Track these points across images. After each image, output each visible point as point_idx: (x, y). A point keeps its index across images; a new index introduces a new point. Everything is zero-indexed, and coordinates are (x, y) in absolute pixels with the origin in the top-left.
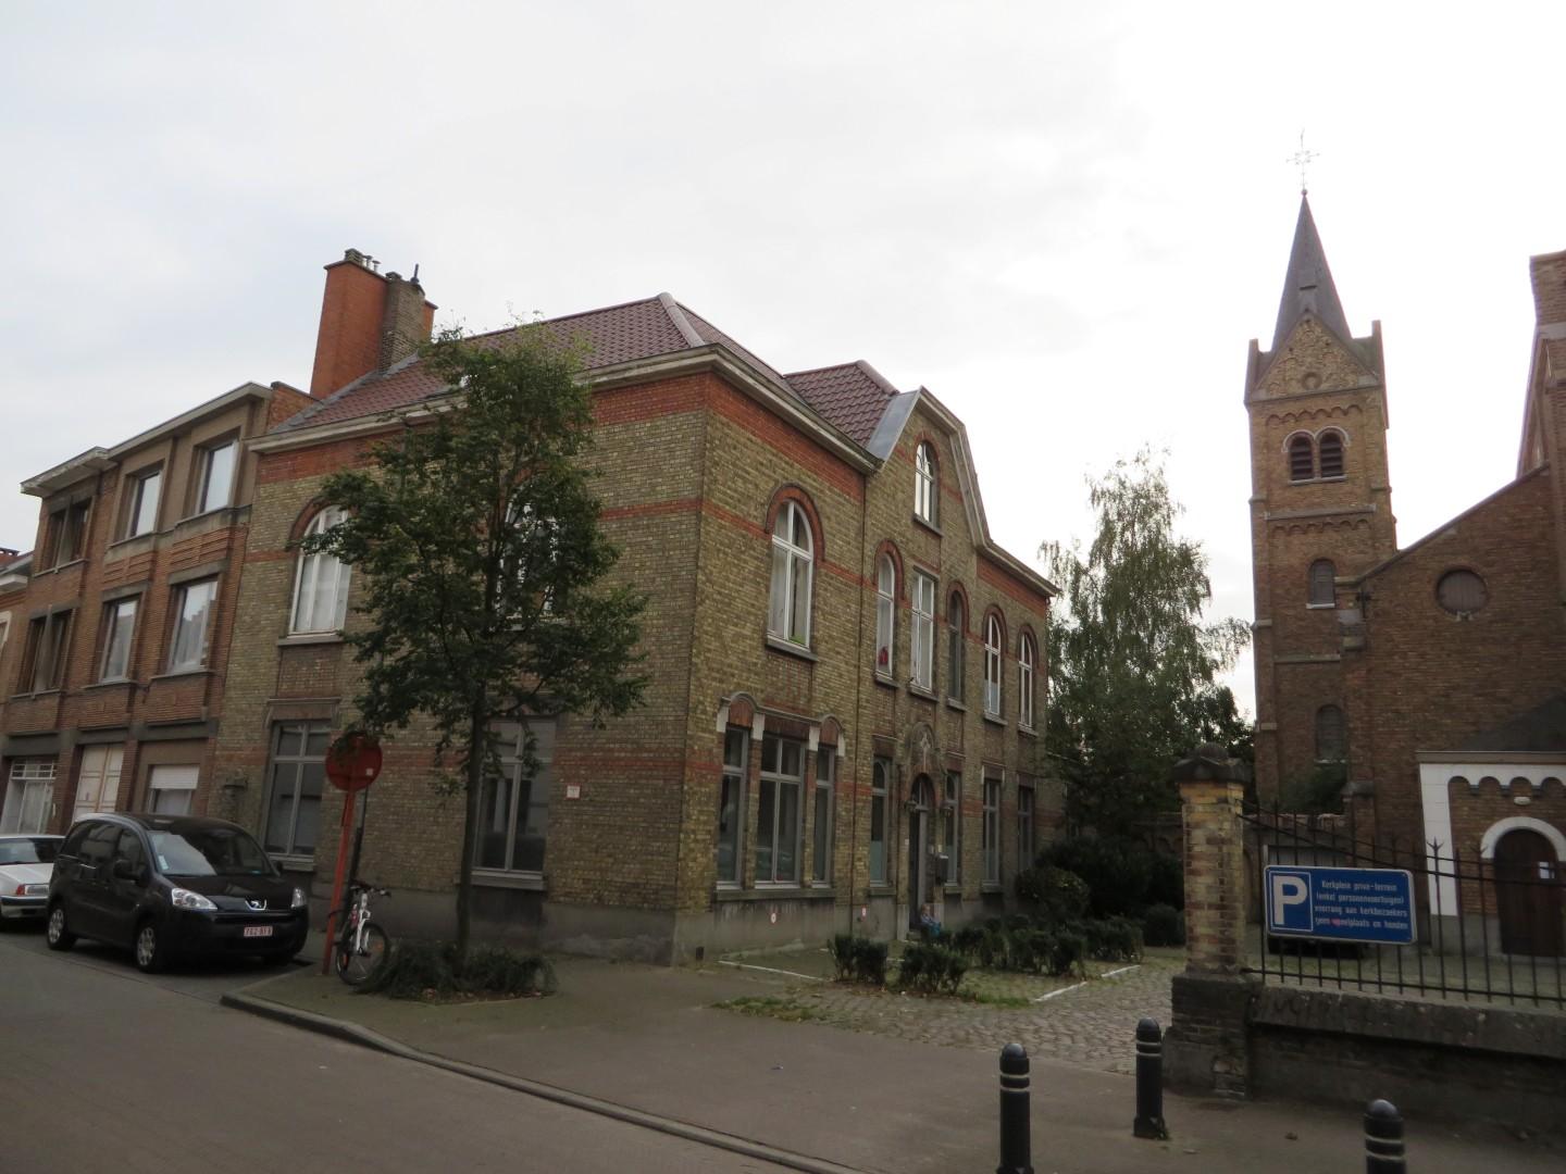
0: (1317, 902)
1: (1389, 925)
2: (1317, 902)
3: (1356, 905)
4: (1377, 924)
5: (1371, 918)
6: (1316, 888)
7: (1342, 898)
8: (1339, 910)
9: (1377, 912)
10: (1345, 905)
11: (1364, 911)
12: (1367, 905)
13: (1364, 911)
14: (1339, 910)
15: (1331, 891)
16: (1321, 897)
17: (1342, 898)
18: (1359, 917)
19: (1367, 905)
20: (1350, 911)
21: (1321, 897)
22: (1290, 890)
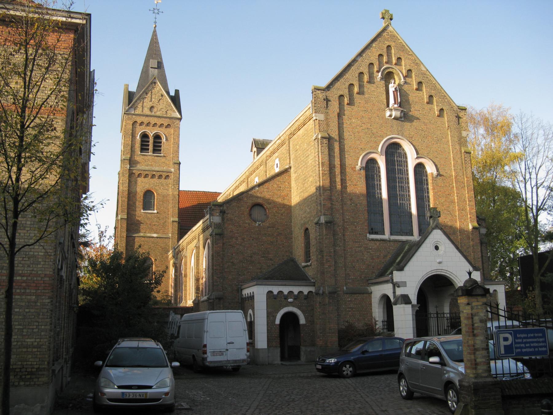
0: (516, 343)
1: (540, 349)
2: (516, 343)
3: (530, 342)
4: (536, 349)
5: (534, 347)
6: (515, 337)
7: (524, 340)
8: (523, 345)
9: (536, 345)
10: (526, 343)
11: (532, 345)
12: (533, 342)
13: (532, 345)
14: (523, 345)
15: (520, 338)
16: (517, 341)
17: (524, 340)
18: (530, 347)
19: (533, 342)
20: (528, 345)
21: (517, 341)
22: (506, 339)
